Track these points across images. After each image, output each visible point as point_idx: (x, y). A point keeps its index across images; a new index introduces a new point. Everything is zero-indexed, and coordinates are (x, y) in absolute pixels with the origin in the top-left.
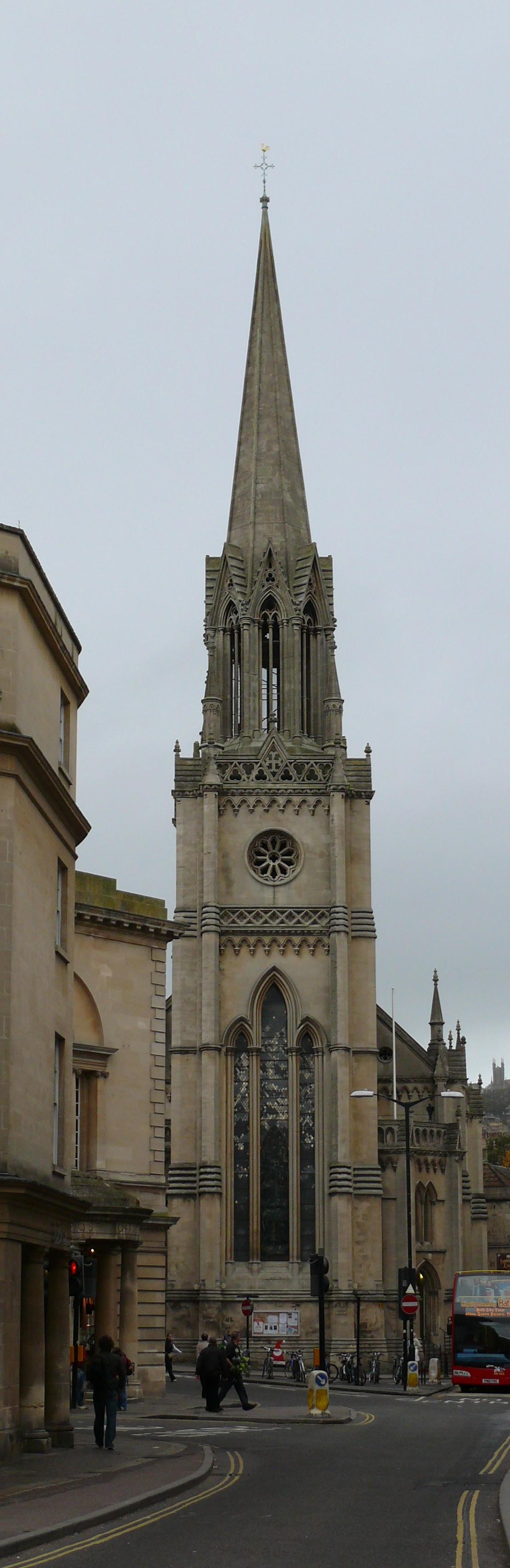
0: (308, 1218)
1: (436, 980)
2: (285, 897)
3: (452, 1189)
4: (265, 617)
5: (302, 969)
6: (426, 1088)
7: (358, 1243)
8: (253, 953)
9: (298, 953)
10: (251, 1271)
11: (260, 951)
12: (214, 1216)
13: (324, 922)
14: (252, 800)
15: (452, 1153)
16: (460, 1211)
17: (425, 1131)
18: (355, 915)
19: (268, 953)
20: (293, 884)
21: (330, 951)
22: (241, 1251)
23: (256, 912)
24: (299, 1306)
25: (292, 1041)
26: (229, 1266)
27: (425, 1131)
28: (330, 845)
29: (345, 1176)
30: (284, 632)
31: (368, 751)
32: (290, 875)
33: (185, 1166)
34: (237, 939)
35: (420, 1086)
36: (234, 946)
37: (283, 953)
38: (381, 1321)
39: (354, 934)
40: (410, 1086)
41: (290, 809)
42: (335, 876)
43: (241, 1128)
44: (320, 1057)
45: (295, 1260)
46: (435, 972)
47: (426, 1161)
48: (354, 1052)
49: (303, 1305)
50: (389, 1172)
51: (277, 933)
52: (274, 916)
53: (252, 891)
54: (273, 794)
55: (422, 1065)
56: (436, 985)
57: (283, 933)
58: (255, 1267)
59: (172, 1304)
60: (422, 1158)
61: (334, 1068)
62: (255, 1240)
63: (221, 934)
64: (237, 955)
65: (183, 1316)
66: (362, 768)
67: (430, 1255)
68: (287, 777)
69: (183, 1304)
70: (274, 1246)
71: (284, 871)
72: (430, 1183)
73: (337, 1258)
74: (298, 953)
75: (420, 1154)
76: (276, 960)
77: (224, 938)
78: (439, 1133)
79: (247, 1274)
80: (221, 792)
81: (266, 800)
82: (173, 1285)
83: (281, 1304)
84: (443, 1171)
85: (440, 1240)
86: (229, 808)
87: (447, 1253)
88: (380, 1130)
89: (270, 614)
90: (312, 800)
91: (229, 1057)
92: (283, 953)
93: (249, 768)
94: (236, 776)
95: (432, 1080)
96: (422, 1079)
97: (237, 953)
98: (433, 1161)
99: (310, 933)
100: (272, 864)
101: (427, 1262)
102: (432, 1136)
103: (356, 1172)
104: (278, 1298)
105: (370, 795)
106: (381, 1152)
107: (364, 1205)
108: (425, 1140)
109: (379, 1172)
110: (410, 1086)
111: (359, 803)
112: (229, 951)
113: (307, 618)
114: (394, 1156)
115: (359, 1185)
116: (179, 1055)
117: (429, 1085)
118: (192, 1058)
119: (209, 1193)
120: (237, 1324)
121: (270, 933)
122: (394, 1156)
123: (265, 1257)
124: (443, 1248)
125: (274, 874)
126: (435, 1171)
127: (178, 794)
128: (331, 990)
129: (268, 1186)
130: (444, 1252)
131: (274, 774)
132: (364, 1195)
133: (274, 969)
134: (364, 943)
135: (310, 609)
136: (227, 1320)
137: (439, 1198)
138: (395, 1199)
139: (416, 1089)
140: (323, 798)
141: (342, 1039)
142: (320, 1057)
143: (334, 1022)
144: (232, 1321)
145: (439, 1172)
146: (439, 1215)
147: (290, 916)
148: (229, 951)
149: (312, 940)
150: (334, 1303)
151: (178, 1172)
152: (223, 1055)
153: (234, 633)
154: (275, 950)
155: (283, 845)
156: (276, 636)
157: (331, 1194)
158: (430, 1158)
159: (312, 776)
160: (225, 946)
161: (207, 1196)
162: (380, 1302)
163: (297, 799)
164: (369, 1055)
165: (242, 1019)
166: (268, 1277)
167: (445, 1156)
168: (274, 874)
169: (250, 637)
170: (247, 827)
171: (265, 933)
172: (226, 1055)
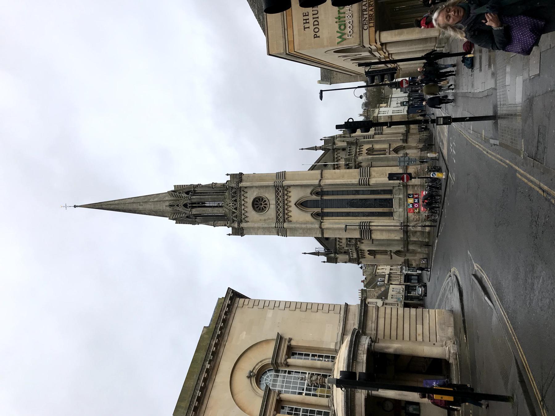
3: (368, 143)
4: (190, 207)
5: (295, 196)
8: (290, 211)
9: (290, 197)
11: (290, 209)
12: (377, 222)
13: (280, 189)
14: (243, 212)
15: (356, 142)
19: (290, 206)
21: (289, 186)
22: (390, 214)
23: (277, 211)
25: (318, 198)
28: (256, 187)
30: (194, 201)
31: (228, 175)
32: (266, 199)
34: (286, 216)
35: (336, 153)
37: (290, 202)
38: (413, 167)
40: (336, 156)
41: (245, 200)
43: (348, 214)
50: (362, 164)
53: (271, 212)
54: (241, 205)
58: (395, 210)
60: (358, 153)
61: (325, 185)
63: (285, 221)
66: (233, 176)
68: (236, 201)
70: (388, 203)
71: (265, 201)
74: (290, 197)
76: (292, 204)
80: (241, 221)
81: (243, 207)
85: (386, 146)
86: (246, 219)
88: (348, 168)
89: (189, 205)
90: (242, 193)
92: (290, 202)
93: (234, 213)
94: (236, 217)
95: (334, 149)
96: (333, 153)
97: (291, 216)
101: (393, 150)
105: (241, 174)
106: (355, 168)
107: (373, 173)
110: (336, 156)
112: (290, 219)
114: (357, 163)
118: (325, 231)
121: (284, 206)
122: (357, 163)
125: (266, 204)
127: (242, 235)
128: (302, 186)
130: (390, 145)
133: (295, 204)
134: (286, 176)
135: (187, 193)
141: (316, 182)
143: (312, 185)
146: (377, 146)
147: (278, 199)
148: (290, 219)
149: (286, 192)
153: (196, 216)
154: (289, 204)
155: (257, 201)
156: (195, 203)
157: (369, 185)
158: (358, 150)
159: (235, 193)
163: (242, 198)
165: (312, 215)
168: (266, 204)
169: (195, 211)
170: (252, 214)
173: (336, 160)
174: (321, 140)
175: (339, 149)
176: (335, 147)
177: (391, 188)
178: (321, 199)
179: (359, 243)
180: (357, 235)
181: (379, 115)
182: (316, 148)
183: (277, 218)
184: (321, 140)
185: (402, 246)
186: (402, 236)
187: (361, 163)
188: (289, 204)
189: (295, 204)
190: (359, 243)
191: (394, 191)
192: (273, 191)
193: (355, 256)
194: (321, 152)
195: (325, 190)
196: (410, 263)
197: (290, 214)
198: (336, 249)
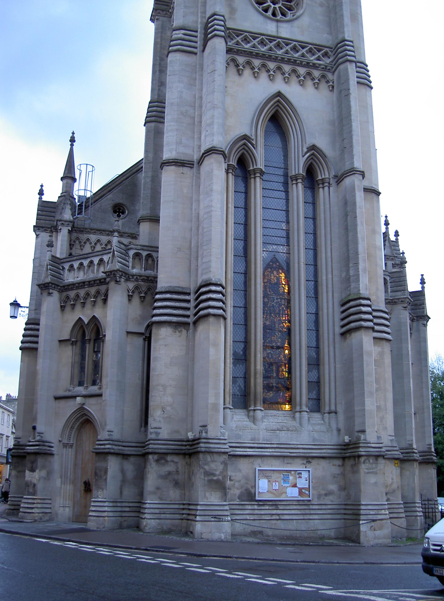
10: (254, 420)
20: (296, 23)
24: (309, 462)
26: (228, 411)
33: (177, 289)
42: (342, 15)
44: (326, 188)
45: (304, 408)
49: (314, 462)
51: (282, 60)
52: (278, 46)
57: (289, 62)
59: (156, 457)
62: (258, 383)
64: (240, 75)
65: (170, 473)
69: (169, 458)
73: (363, 404)
79: (247, 423)
83: (290, 460)
91: (230, 175)
99: (315, 66)
100: (273, 6)
104: (286, 452)
116: (173, 167)
119: (215, 315)
120: (237, 484)
123: (271, 404)
133: (279, 94)
142: (326, 188)
150: (362, 459)
151: (168, 296)
161: (211, 319)
165: (245, 137)
166: (274, 427)
171: (270, 58)
178: (295, 178)
179: (131, 285)
180: (163, 282)
183: (238, 32)
185: (116, 436)
186: (165, 434)
188: (279, 78)
189: (279, 94)
190: (131, 285)
192: (322, 38)
193: (70, 278)
195: (322, 193)
196: (40, 461)
197: (247, 72)
198: (82, 230)
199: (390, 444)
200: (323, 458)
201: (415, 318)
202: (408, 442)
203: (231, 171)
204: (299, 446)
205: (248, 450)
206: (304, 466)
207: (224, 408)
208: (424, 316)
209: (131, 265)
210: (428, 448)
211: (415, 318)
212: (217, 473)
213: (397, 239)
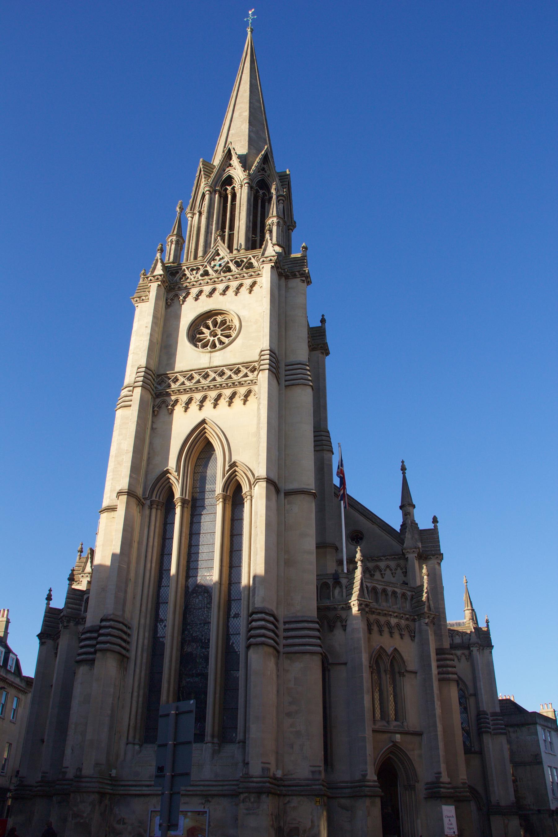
0: (229, 688)
1: (403, 469)
2: (220, 358)
6: (398, 565)
7: (289, 715)
16: (435, 684)
17: (384, 591)
18: (288, 368)
24: (209, 801)
27: (384, 591)
29: (263, 623)
35: (392, 564)
36: (167, 406)
39: (287, 383)
40: (382, 565)
46: (403, 462)
47: (388, 624)
48: (288, 494)
50: (338, 633)
55: (394, 543)
56: (404, 473)
60: (382, 619)
67: (398, 736)
72: (395, 649)
75: (379, 614)
77: (158, 401)
78: (404, 595)
82: (65, 773)
84: (413, 638)
85: (413, 719)
87: (425, 736)
89: (229, 188)
91: (154, 511)
95: (403, 556)
98: (398, 625)
100: (212, 339)
102: (396, 597)
103: (287, 626)
108: (387, 601)
109: (317, 626)
110: (382, 565)
111: (296, 283)
113: (261, 192)
115: (290, 641)
117: (402, 562)
124: (418, 729)
126: (402, 636)
129: (189, 650)
130: (419, 734)
131: (216, 271)
132: (295, 653)
133: (204, 422)
136: (118, 822)
137: (409, 668)
138: (345, 664)
139: (388, 567)
140: (258, 279)
144: (124, 823)
145: (407, 638)
152: (146, 507)
158: (393, 621)
160: (159, 407)
162: (269, 793)
164: (302, 496)
167: (414, 620)
171: (197, 390)
172: (151, 508)
173: (370, 565)
174: (435, 520)
175: (405, 573)
176: (412, 556)
177: (240, 737)
181: (539, 728)
182: (407, 505)
184: (435, 520)
187: (344, 627)
191: (232, 749)
194: (395, 521)
199: (311, 777)
200: (224, 796)
201: (416, 617)
202: (362, 773)
203: (155, 506)
204: (198, 783)
205: (144, 788)
206: (203, 806)
207: (127, 744)
208: (423, 614)
209: (83, 610)
210: (436, 777)
211: (416, 617)
212: (85, 815)
213: (436, 527)
